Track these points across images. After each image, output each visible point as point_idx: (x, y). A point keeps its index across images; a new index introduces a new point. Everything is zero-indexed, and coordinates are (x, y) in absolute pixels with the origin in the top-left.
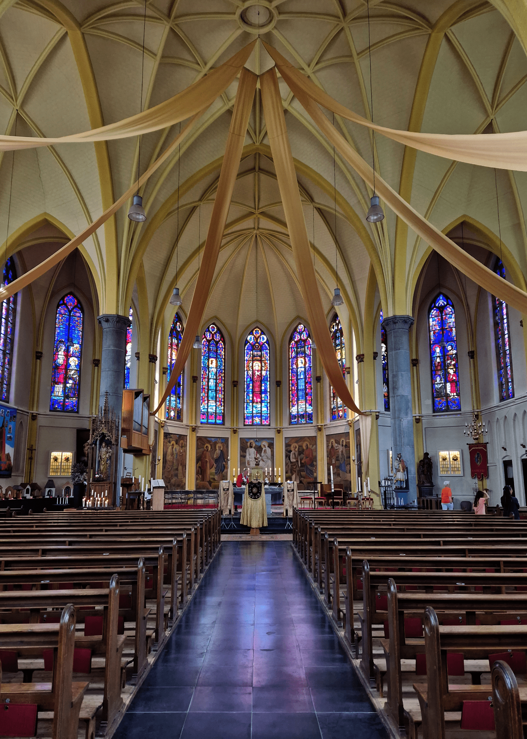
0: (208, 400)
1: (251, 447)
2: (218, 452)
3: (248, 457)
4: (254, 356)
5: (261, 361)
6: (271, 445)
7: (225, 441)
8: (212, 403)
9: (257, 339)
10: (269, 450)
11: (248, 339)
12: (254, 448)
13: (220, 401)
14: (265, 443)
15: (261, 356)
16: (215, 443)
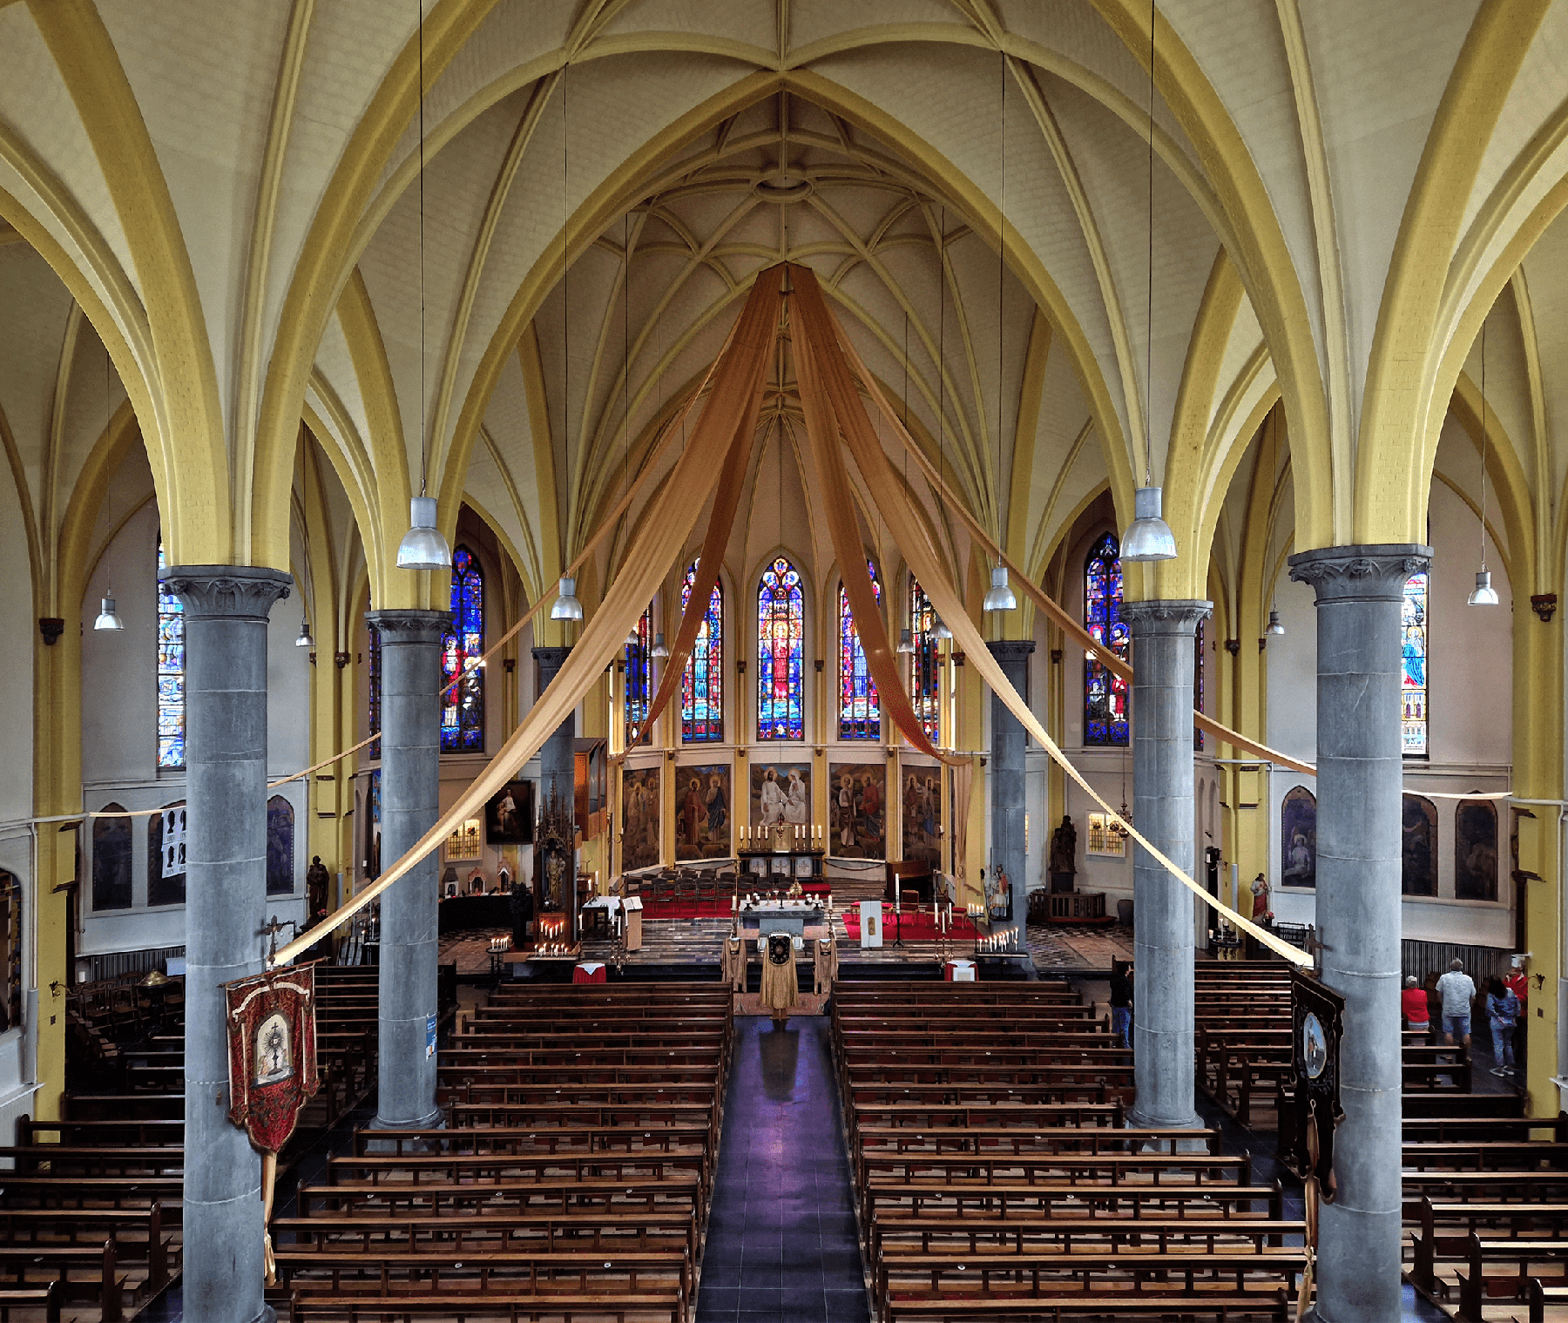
0: (694, 699)
1: (770, 779)
2: (713, 790)
3: (764, 797)
4: (774, 612)
5: (787, 620)
6: (806, 777)
7: (725, 770)
8: (701, 703)
9: (780, 579)
10: (802, 786)
11: (765, 579)
12: (778, 782)
13: (715, 699)
14: (795, 772)
15: (787, 612)
16: (708, 776)
